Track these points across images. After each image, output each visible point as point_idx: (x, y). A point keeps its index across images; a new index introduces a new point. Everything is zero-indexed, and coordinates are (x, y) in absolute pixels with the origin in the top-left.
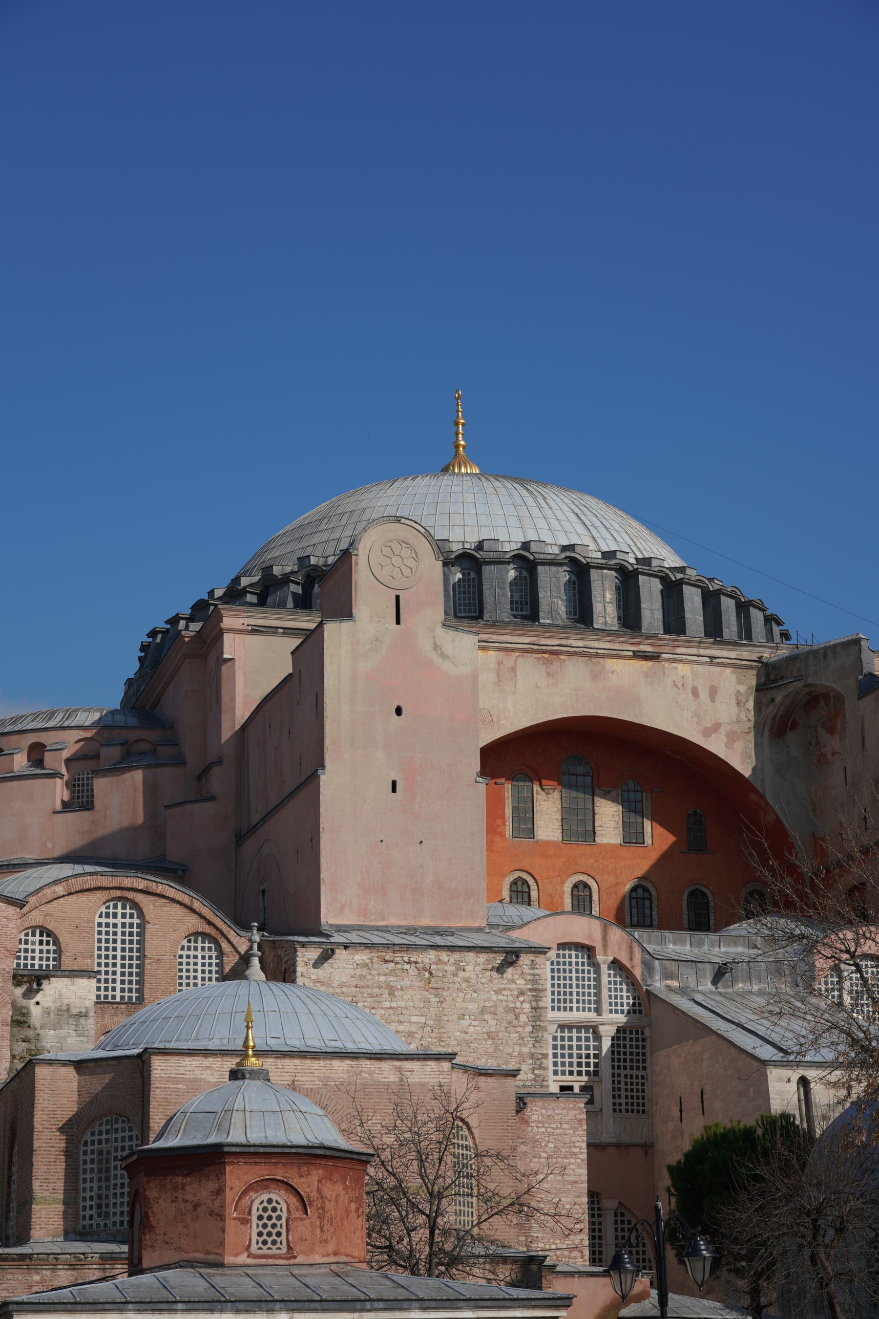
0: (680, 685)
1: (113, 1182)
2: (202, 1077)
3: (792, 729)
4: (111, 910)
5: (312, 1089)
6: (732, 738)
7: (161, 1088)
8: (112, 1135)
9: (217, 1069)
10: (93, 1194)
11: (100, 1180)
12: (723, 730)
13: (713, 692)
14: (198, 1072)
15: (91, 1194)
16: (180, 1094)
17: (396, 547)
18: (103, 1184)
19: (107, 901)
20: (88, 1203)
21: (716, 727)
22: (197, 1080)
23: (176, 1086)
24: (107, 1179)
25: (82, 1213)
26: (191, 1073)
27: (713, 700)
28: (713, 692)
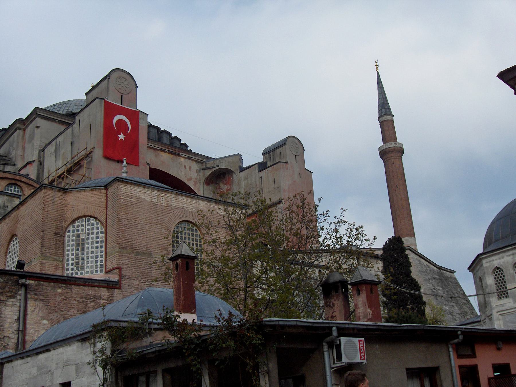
0: (181, 164)
1: (86, 250)
2: (143, 197)
3: (212, 183)
4: (10, 188)
5: (191, 212)
6: (195, 184)
7: (123, 199)
8: (85, 227)
9: (150, 195)
10: (74, 257)
11: (78, 250)
12: (193, 180)
13: (190, 168)
14: (140, 194)
15: (72, 257)
16: (132, 203)
17: (123, 80)
18: (80, 252)
19: (9, 184)
20: (70, 262)
21: (191, 179)
22: (140, 198)
23: (130, 199)
24: (83, 249)
25: (66, 267)
26: (137, 194)
27: (190, 170)
28: (190, 168)
